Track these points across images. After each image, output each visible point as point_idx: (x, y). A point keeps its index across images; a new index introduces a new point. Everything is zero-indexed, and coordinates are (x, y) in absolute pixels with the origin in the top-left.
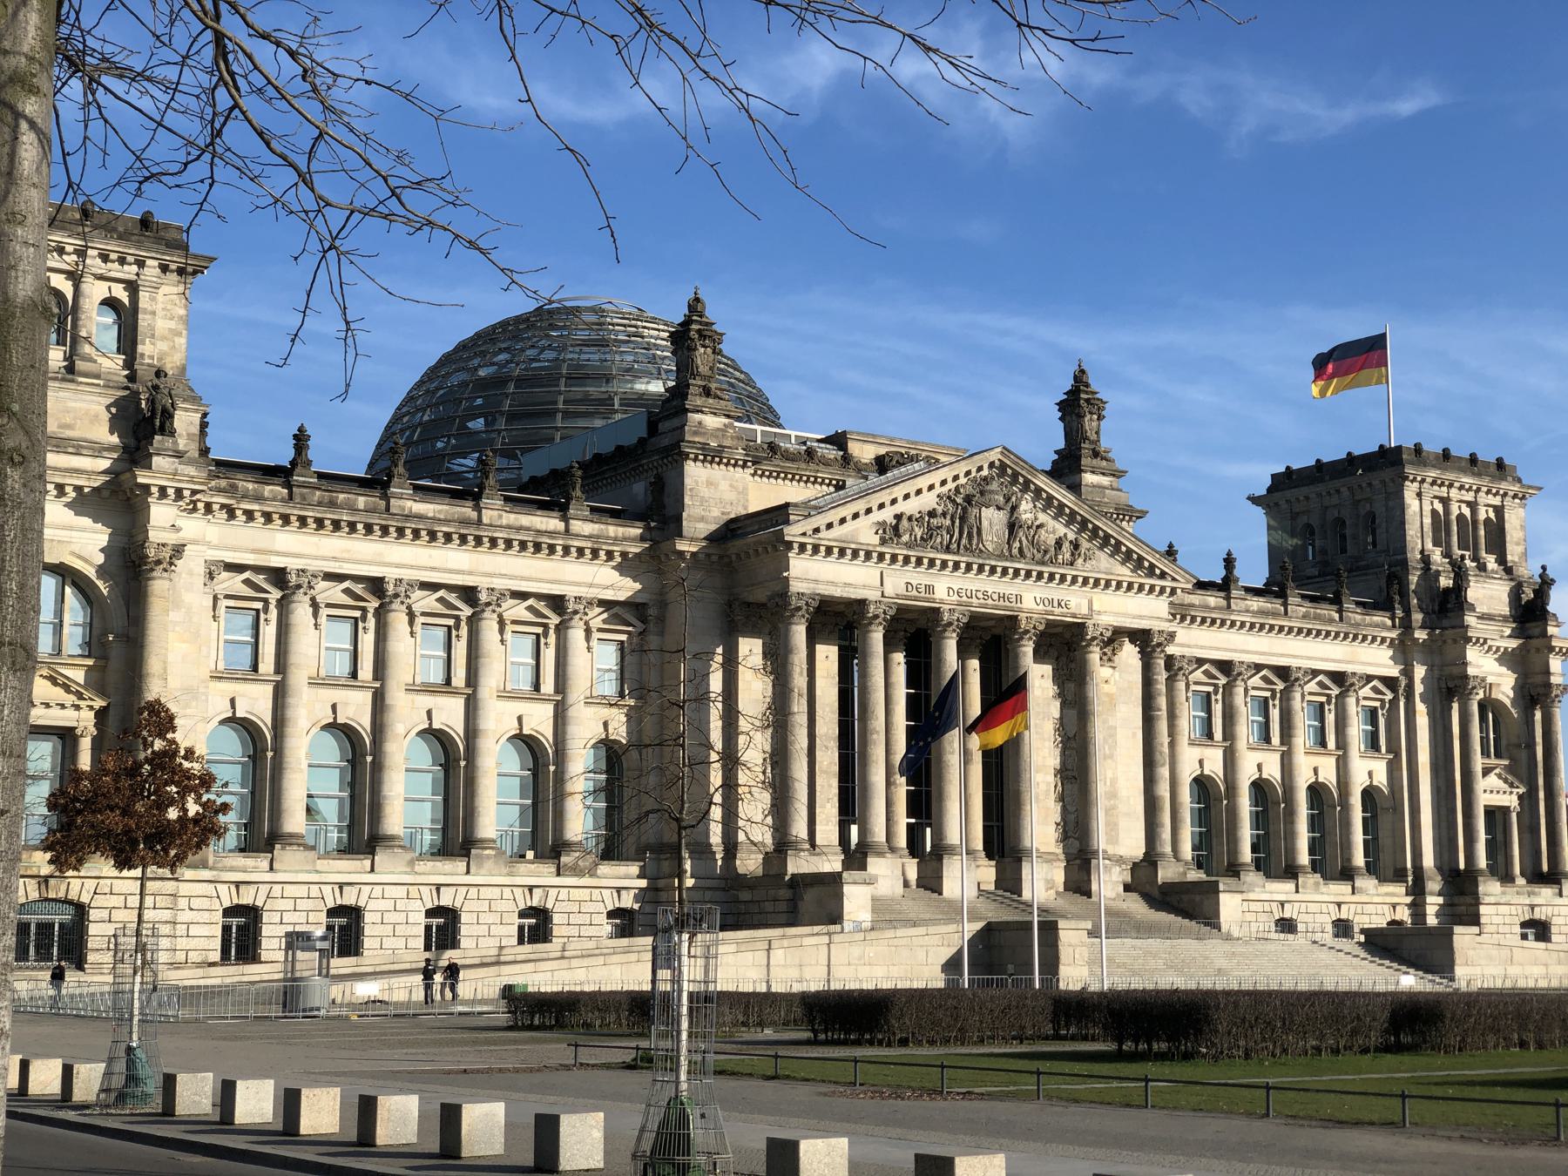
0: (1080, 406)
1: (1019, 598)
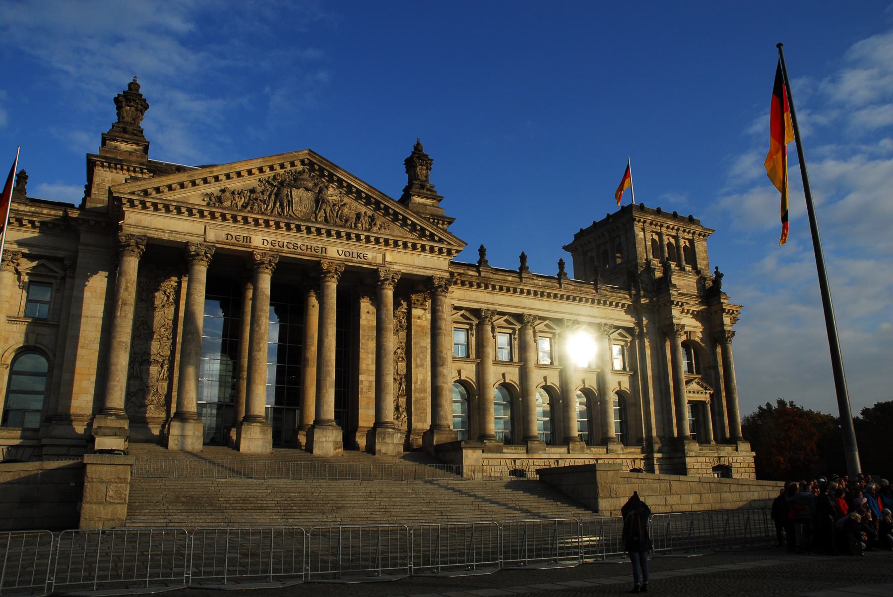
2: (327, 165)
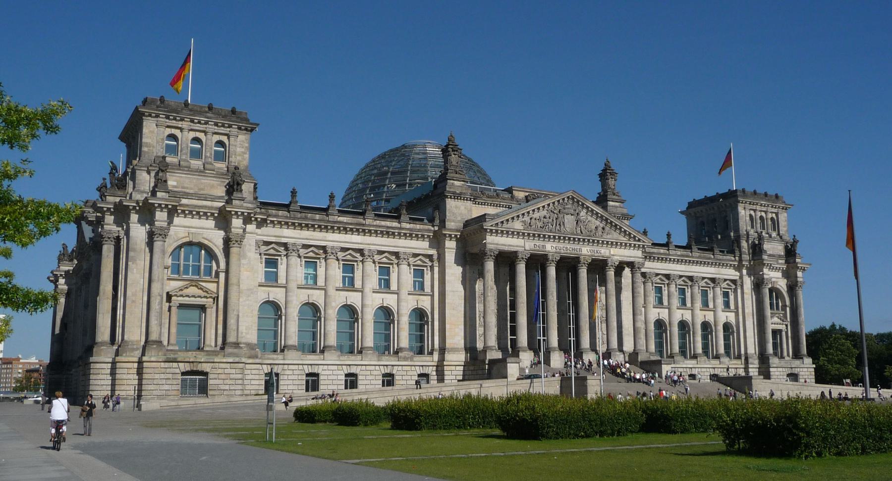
0: (607, 175)
1: (580, 250)
2: (581, 199)
